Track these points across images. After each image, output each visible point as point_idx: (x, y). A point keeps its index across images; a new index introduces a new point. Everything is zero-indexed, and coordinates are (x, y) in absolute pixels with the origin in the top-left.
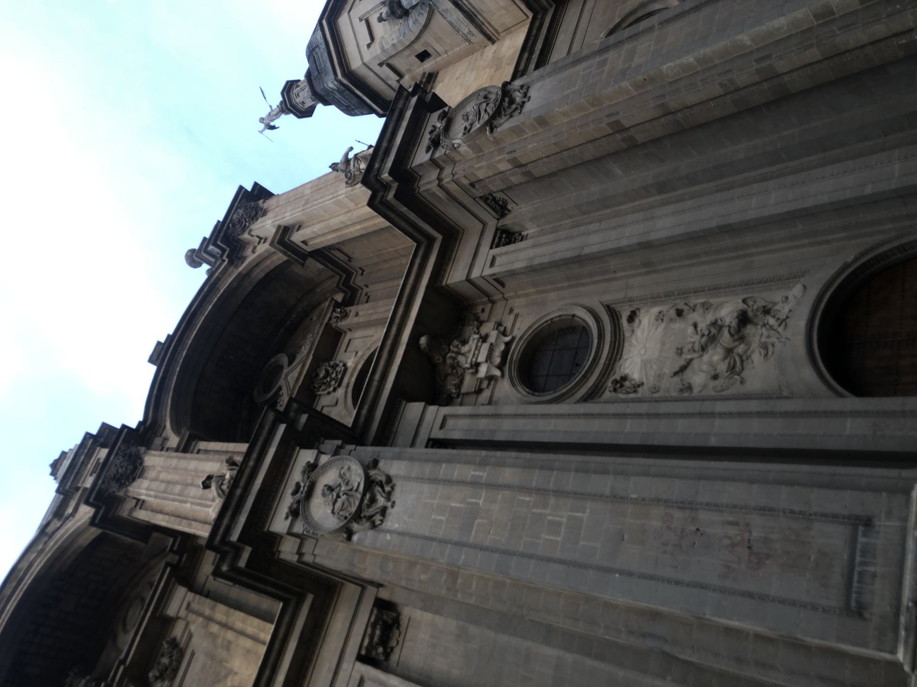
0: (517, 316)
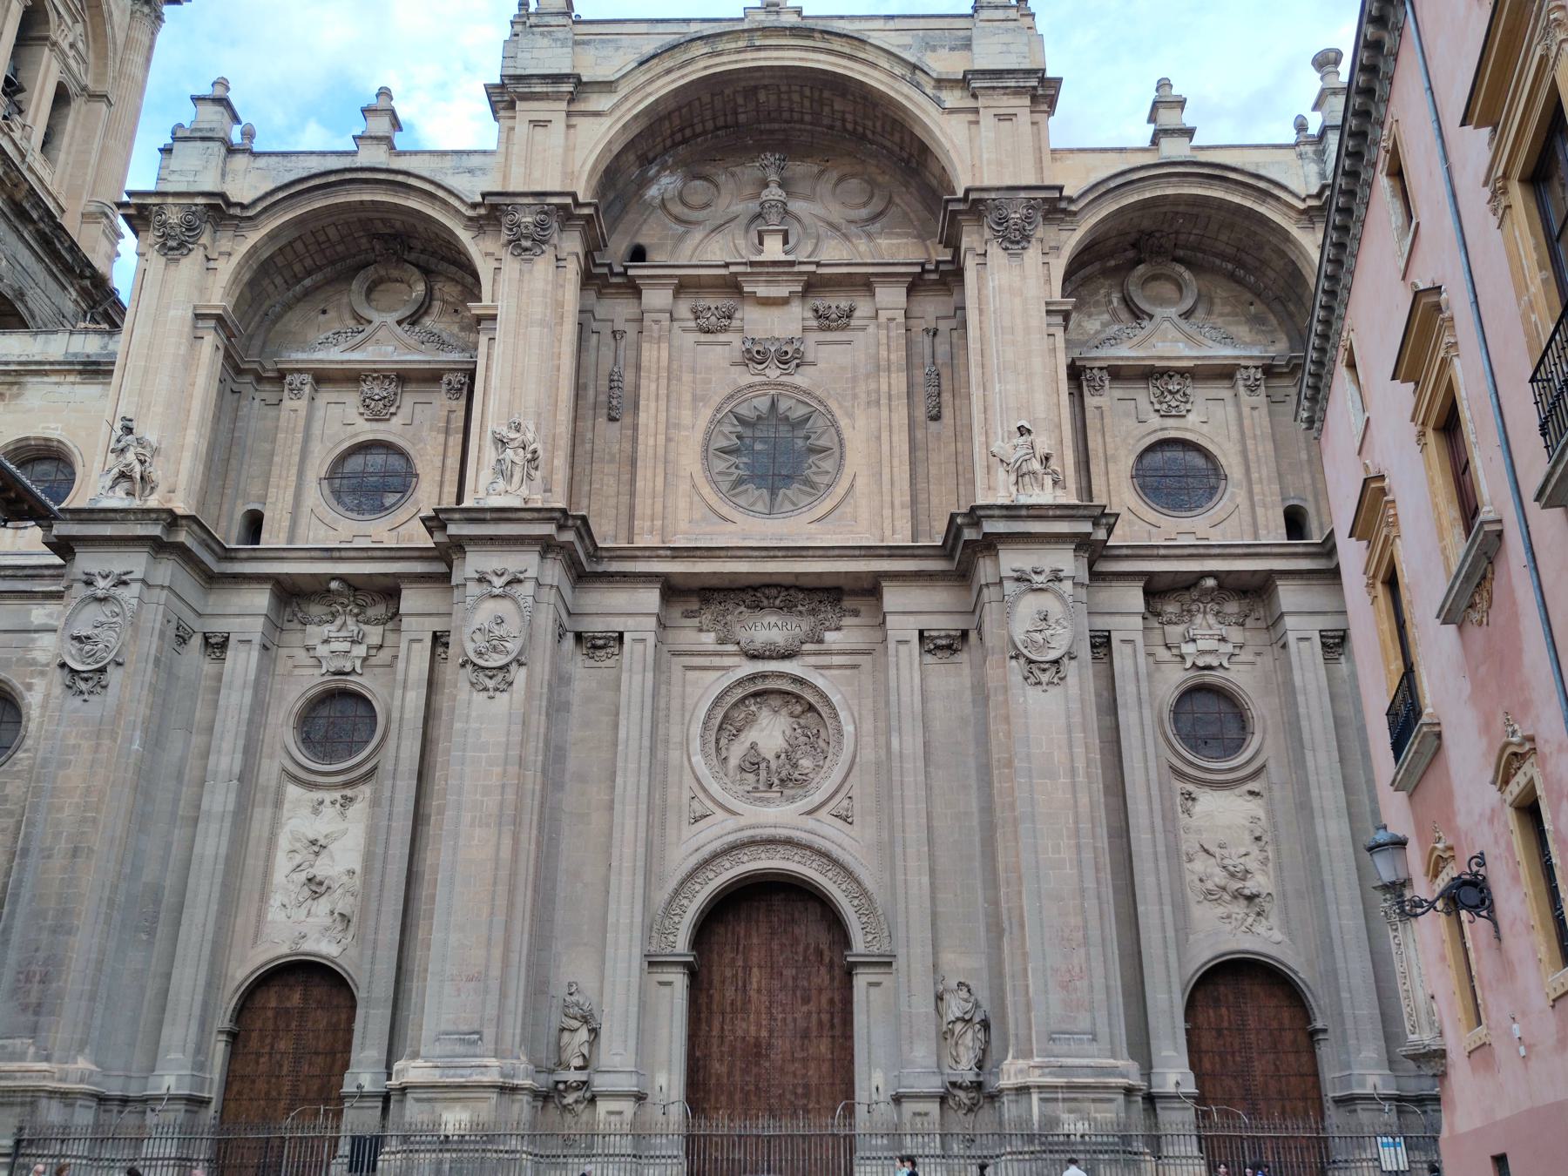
0: (1253, 663)
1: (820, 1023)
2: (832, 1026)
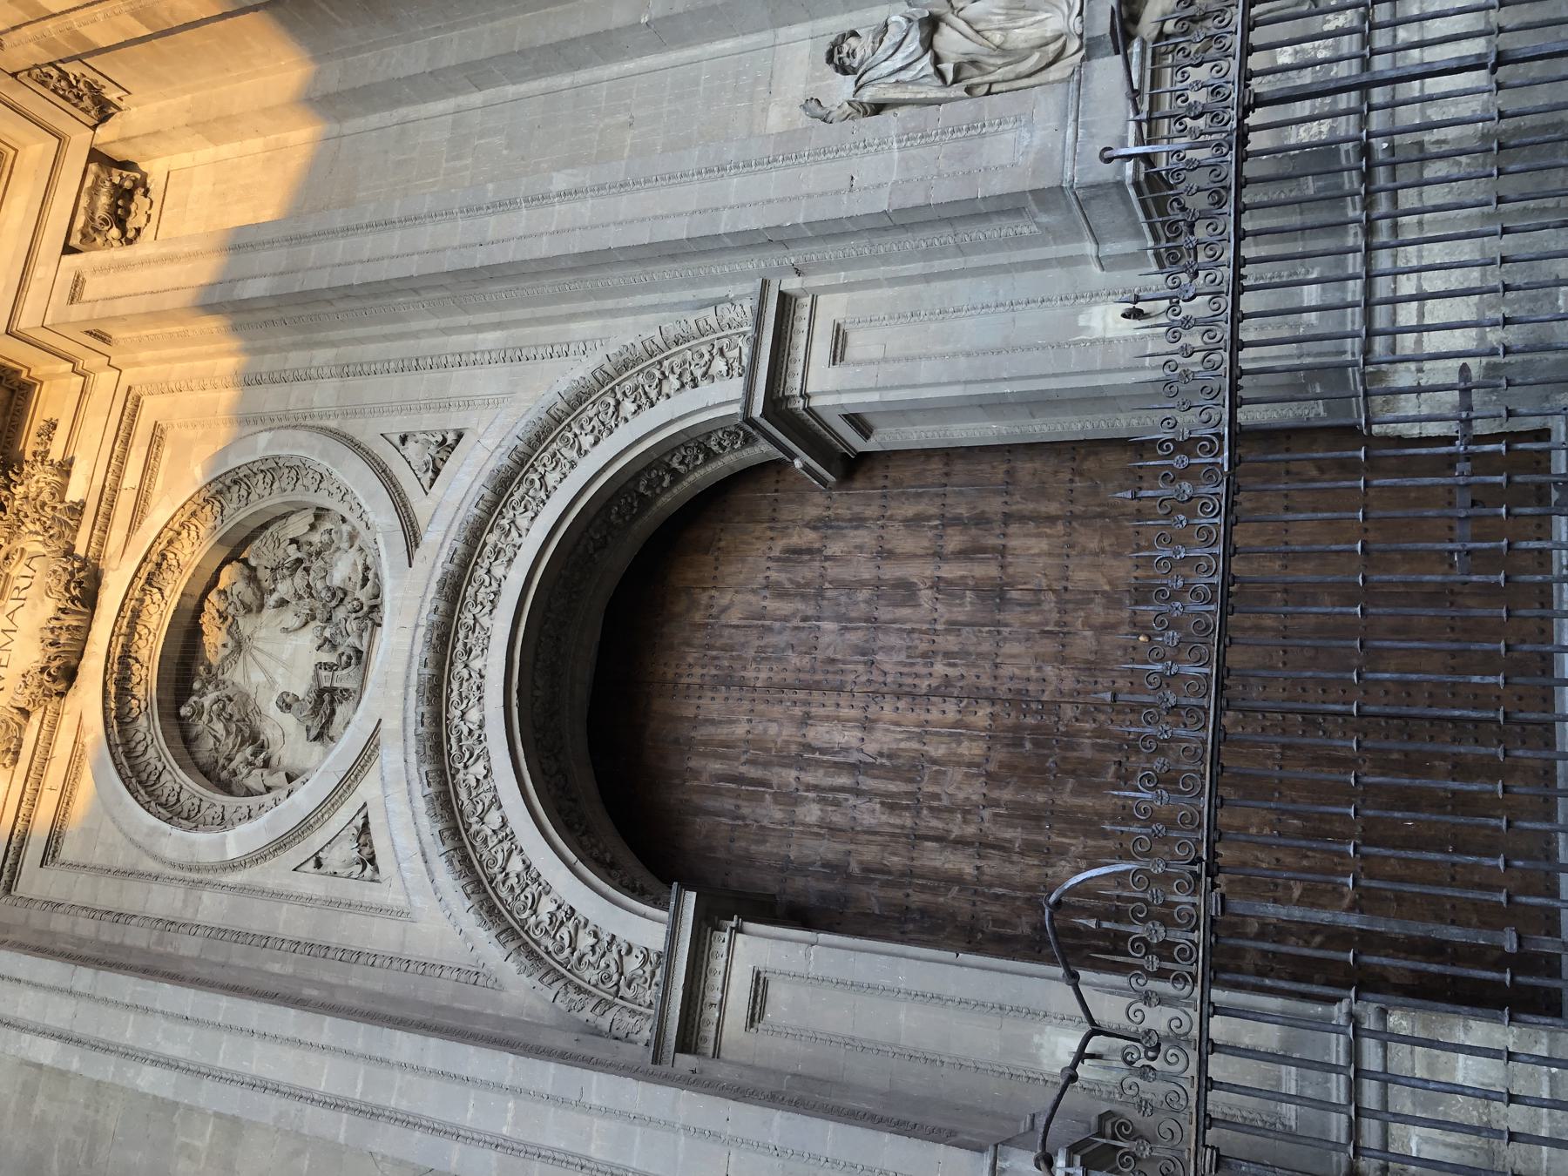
1: (965, 554)
2: (981, 521)
